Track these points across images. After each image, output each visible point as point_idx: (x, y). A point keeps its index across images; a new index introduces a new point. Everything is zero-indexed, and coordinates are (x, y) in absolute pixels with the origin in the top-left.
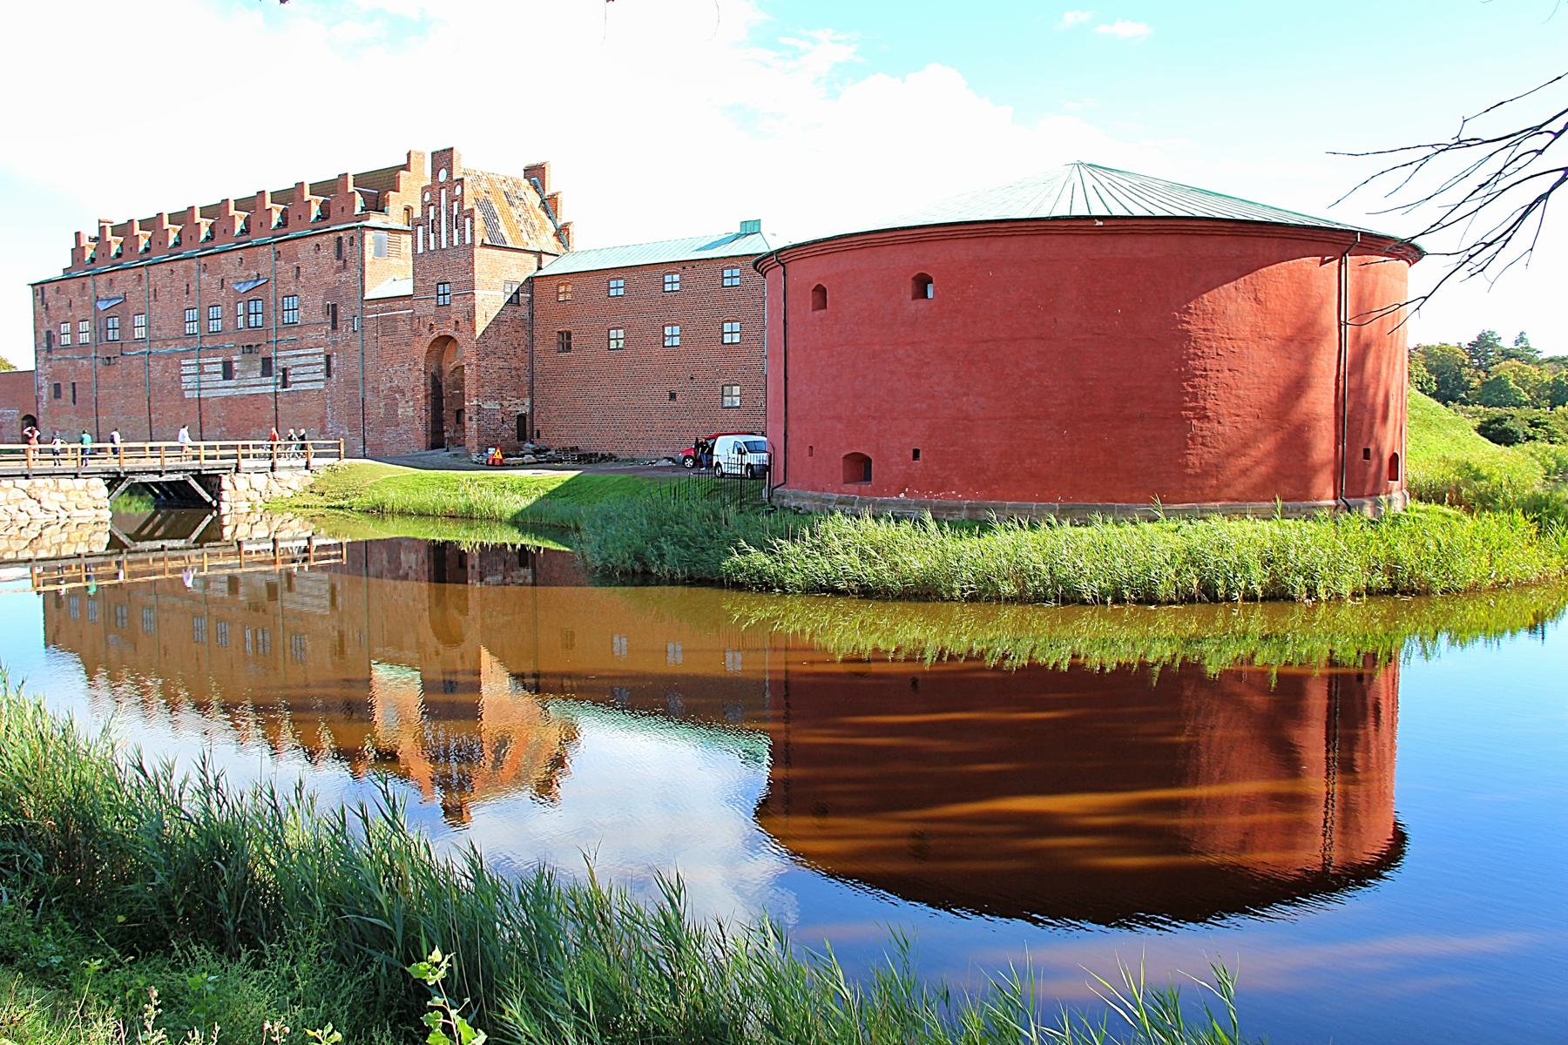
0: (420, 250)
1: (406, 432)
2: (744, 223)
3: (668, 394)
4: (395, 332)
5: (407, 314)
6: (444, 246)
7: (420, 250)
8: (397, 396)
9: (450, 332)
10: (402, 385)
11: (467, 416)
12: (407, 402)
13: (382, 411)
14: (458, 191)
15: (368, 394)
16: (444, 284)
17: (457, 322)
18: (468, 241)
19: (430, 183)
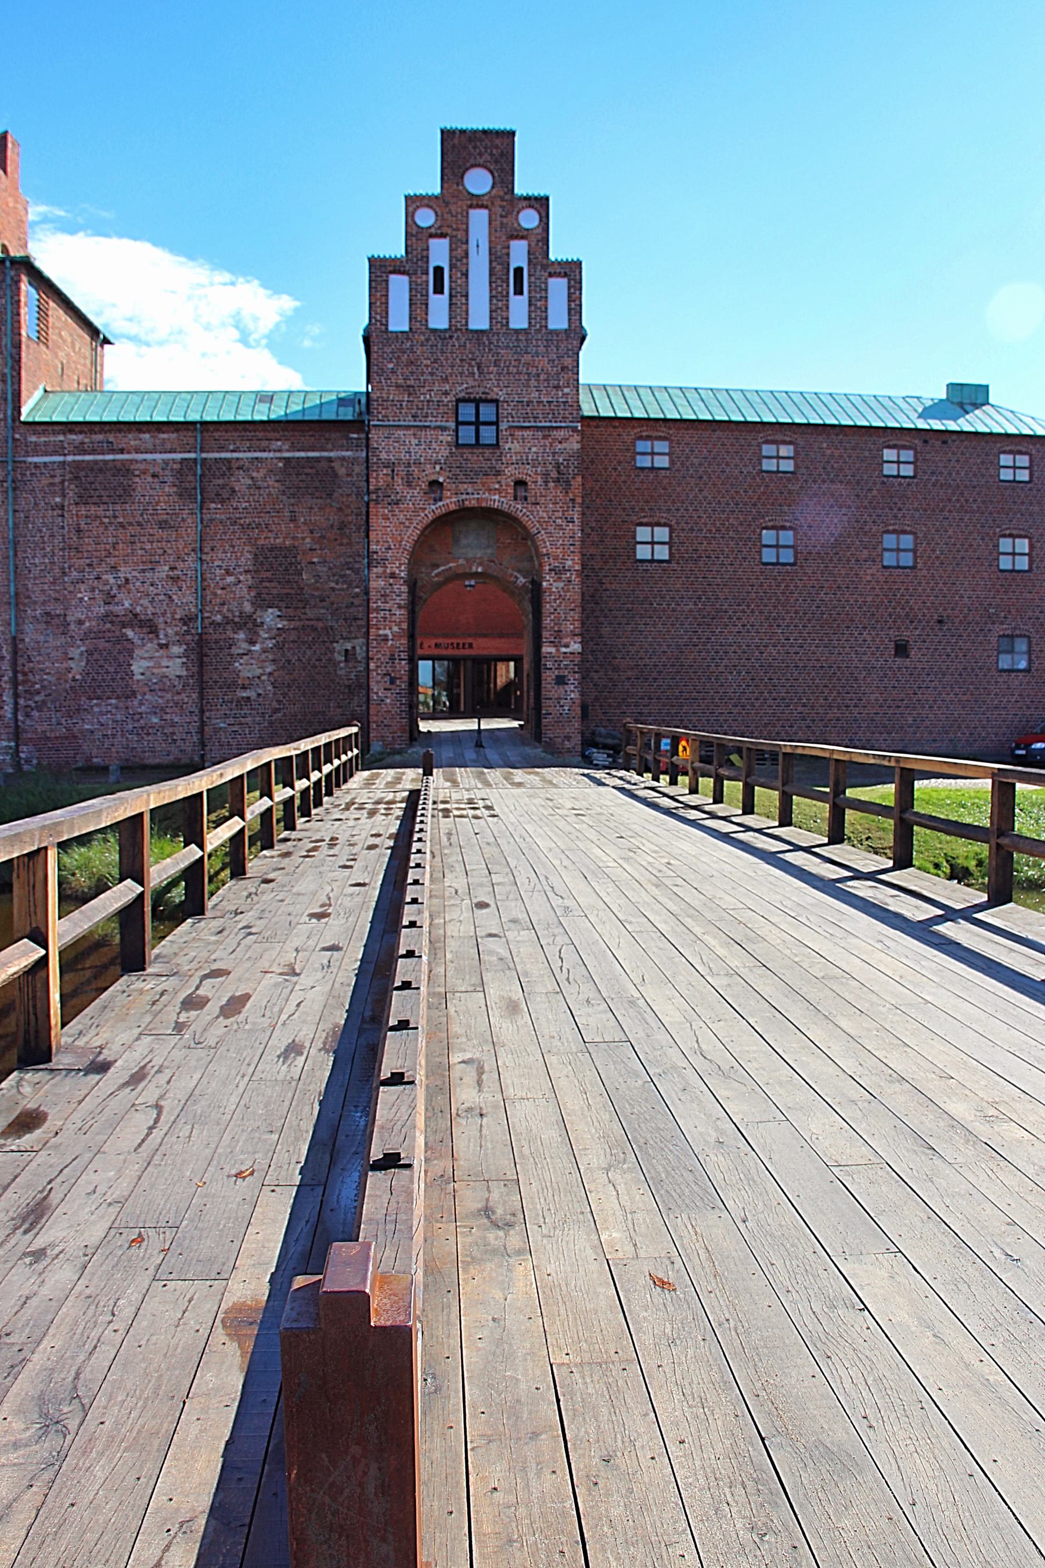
0: (399, 321)
1: (155, 710)
2: (953, 388)
3: (892, 645)
4: (125, 494)
5: (166, 462)
6: (479, 319)
7: (399, 321)
8: (130, 633)
9: (496, 501)
10: (145, 608)
11: (548, 677)
12: (166, 646)
13: (77, 667)
14: (529, 219)
15: (28, 628)
16: (477, 402)
17: (520, 483)
18: (558, 320)
19: (434, 188)
